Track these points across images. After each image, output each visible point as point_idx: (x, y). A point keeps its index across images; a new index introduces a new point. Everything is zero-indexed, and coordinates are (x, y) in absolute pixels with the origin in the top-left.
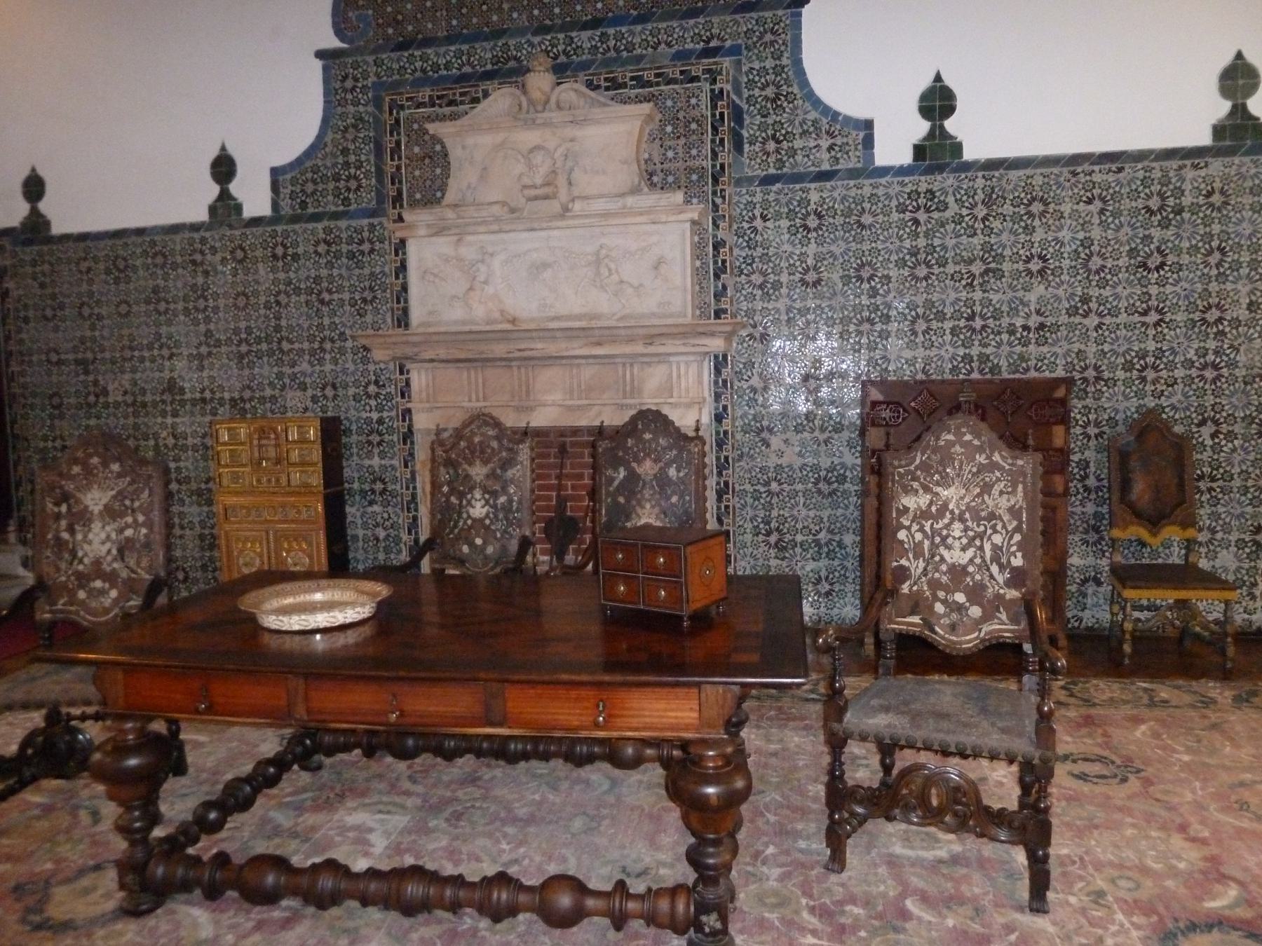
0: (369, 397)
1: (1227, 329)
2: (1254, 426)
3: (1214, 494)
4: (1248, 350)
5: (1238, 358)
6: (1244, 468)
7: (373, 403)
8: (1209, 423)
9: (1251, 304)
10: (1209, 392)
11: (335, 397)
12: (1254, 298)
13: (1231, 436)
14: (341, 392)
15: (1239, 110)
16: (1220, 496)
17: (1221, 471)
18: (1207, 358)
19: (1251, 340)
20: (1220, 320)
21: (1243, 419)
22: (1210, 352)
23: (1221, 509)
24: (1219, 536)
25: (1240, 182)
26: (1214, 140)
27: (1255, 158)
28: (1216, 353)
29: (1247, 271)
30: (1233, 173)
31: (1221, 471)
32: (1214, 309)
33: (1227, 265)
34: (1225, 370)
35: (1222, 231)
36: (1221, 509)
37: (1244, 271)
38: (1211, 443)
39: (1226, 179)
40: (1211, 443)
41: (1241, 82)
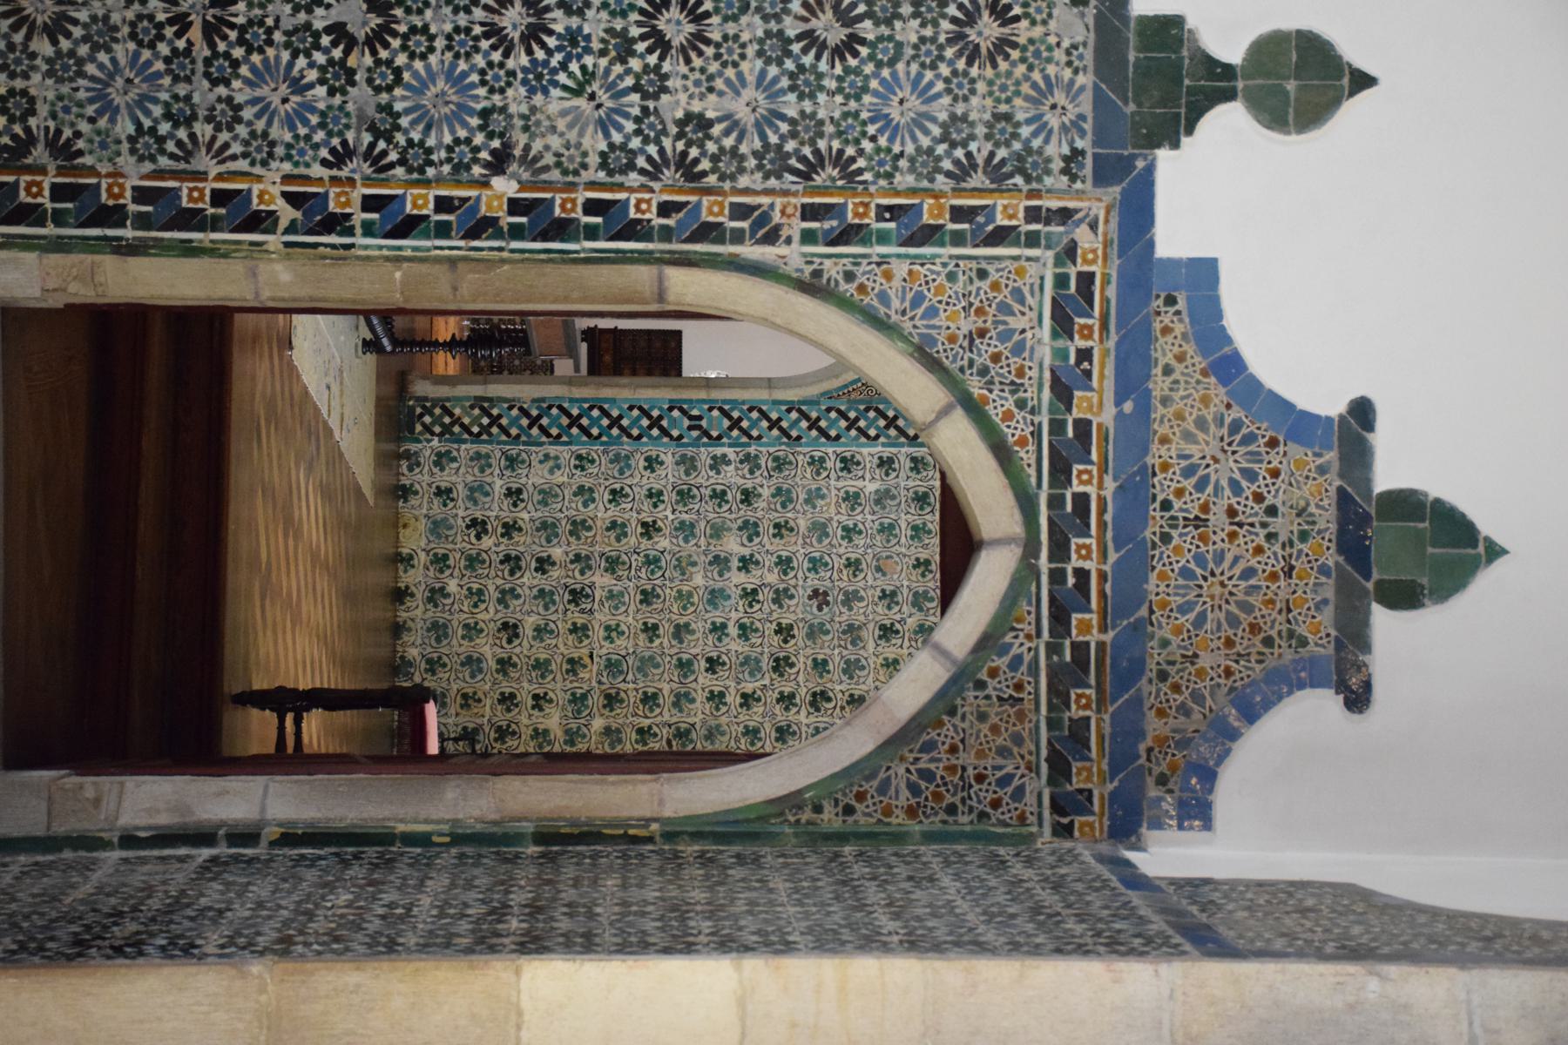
1: (635, 64)
2: (367, 138)
3: (169, 32)
4: (577, 120)
5: (556, 93)
6: (247, 114)
8: (375, 21)
9: (704, 124)
10: (462, 20)
12: (716, 130)
13: (340, 77)
15: (1217, 83)
16: (163, 48)
17: (238, 53)
18: (558, 14)
19: (604, 126)
20: (661, 44)
21: (387, 109)
22: (574, 22)
23: (123, 50)
24: (43, 46)
25: (1025, 88)
26: (1143, 20)
27: (1088, 126)
28: (572, 37)
29: (792, 113)
30: (1051, 70)
31: (238, 53)
32: (690, 28)
33: (808, 60)
34: (524, 60)
35: (899, 46)
36: (123, 50)
37: (791, 106)
38: (318, 25)
39: (1036, 54)
40: (318, 25)
41: (1291, 86)
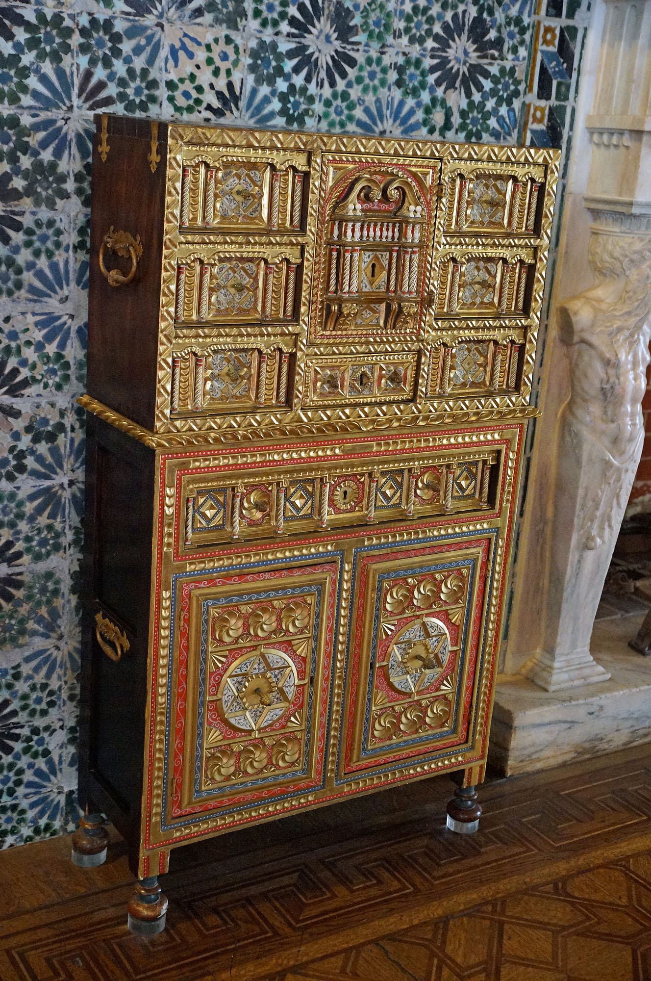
0: (449, 79)
7: (457, 100)
11: (341, 62)
14: (363, 49)
